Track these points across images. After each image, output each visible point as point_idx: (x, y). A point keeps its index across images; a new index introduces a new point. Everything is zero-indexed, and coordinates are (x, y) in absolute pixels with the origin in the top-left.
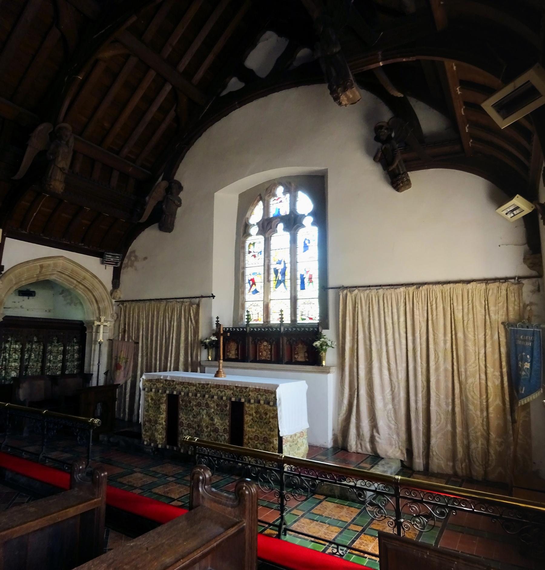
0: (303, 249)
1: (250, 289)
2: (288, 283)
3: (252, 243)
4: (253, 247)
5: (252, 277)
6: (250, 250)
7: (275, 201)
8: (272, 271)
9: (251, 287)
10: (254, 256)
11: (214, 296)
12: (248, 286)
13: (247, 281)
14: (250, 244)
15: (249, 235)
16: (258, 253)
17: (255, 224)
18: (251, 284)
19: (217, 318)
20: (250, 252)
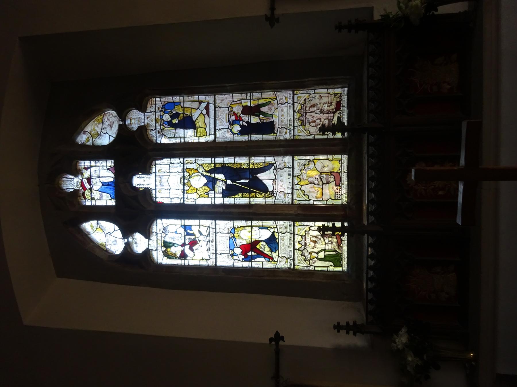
0: (190, 132)
1: (266, 256)
2: (258, 160)
3: (164, 249)
4: (173, 248)
5: (238, 251)
6: (178, 255)
7: (87, 193)
8: (229, 201)
9: (261, 254)
10: (193, 243)
11: (277, 334)
12: (259, 263)
13: (246, 264)
14: (166, 254)
15: (147, 252)
16: (188, 234)
17: (126, 240)
18: (253, 253)
19: (338, 331)
20: (183, 256)
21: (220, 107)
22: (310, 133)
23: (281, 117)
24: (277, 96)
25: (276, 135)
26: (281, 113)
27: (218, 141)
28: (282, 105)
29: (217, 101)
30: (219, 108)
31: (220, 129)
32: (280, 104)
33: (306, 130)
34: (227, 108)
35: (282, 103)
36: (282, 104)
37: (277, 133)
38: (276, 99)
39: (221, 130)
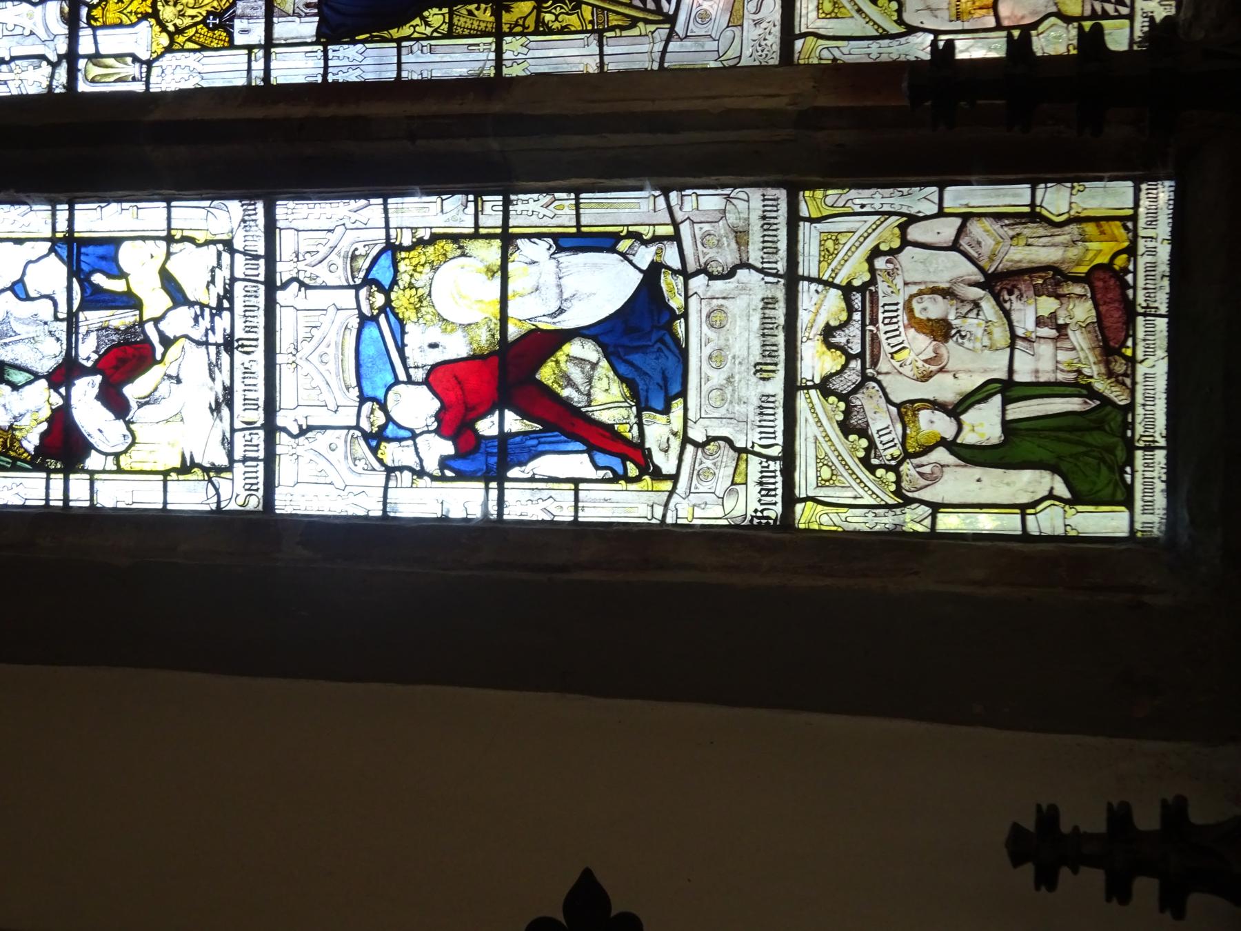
21: (302, 284)
22: (898, 492)
23: (705, 367)
24: (679, 216)
25: (668, 485)
26: (709, 341)
27: (289, 510)
28: (718, 285)
29: (286, 243)
30: (295, 285)
31: (303, 432)
32: (702, 278)
33: (872, 469)
34: (349, 287)
35: (715, 269)
36: (712, 277)
37: (675, 478)
38: (676, 238)
39: (309, 435)
